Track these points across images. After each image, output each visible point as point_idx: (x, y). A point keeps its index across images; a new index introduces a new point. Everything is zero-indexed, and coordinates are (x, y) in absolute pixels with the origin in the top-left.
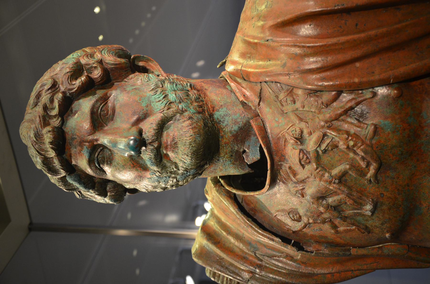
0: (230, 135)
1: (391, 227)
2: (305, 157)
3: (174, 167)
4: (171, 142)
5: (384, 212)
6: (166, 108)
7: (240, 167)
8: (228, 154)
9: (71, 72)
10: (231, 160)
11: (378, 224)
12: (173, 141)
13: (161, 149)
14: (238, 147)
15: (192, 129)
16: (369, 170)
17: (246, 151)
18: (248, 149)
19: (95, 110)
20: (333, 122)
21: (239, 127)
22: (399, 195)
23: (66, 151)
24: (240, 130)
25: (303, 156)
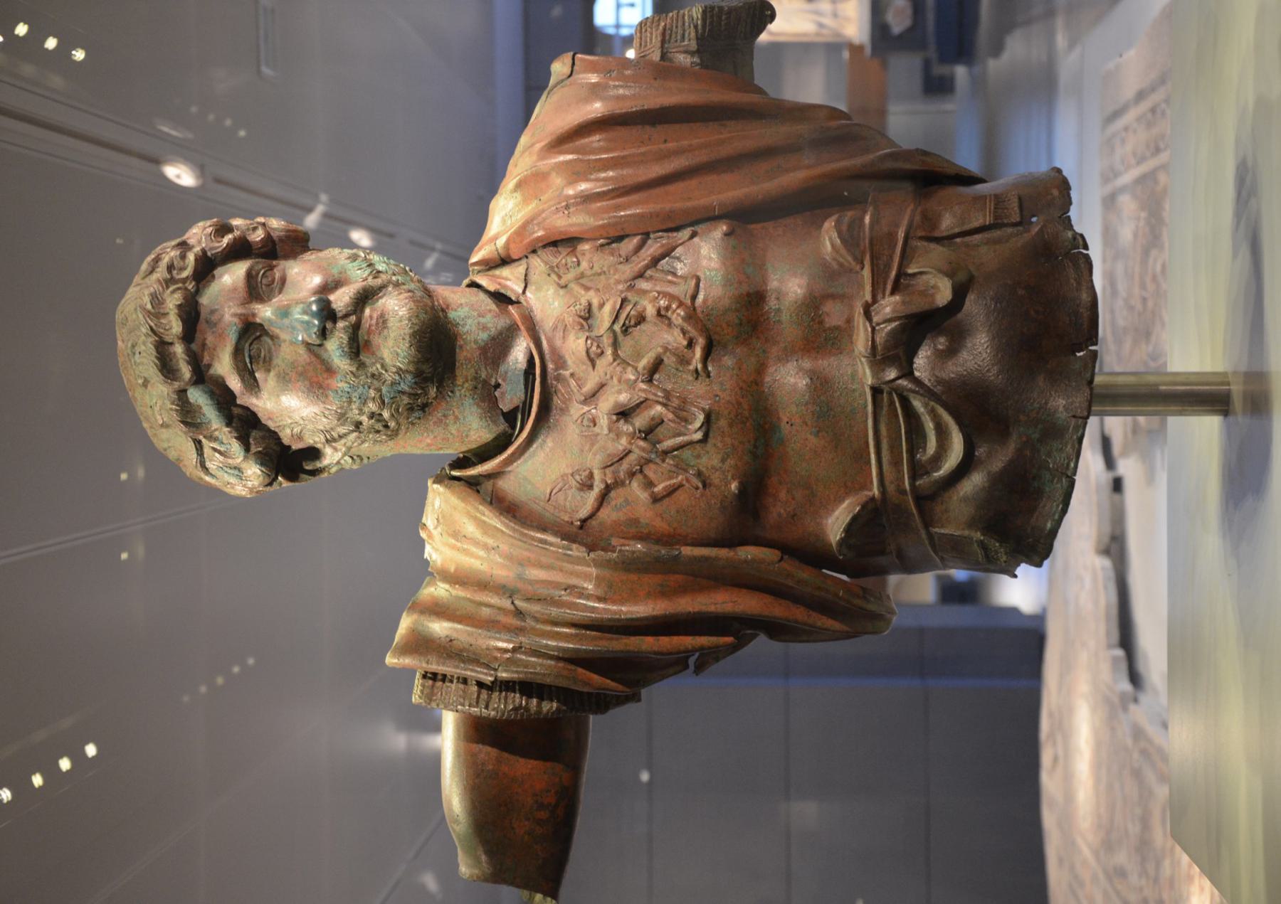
0: (475, 346)
1: (736, 465)
2: (595, 344)
3: (379, 366)
5: (723, 432)
6: (370, 278)
8: (470, 382)
9: (216, 225)
10: (473, 397)
11: (716, 462)
13: (360, 332)
14: (488, 372)
15: (414, 301)
16: (694, 352)
18: (504, 380)
19: (254, 273)
20: (636, 281)
21: (489, 336)
22: (743, 398)
23: (198, 335)
24: (491, 340)
25: (592, 344)
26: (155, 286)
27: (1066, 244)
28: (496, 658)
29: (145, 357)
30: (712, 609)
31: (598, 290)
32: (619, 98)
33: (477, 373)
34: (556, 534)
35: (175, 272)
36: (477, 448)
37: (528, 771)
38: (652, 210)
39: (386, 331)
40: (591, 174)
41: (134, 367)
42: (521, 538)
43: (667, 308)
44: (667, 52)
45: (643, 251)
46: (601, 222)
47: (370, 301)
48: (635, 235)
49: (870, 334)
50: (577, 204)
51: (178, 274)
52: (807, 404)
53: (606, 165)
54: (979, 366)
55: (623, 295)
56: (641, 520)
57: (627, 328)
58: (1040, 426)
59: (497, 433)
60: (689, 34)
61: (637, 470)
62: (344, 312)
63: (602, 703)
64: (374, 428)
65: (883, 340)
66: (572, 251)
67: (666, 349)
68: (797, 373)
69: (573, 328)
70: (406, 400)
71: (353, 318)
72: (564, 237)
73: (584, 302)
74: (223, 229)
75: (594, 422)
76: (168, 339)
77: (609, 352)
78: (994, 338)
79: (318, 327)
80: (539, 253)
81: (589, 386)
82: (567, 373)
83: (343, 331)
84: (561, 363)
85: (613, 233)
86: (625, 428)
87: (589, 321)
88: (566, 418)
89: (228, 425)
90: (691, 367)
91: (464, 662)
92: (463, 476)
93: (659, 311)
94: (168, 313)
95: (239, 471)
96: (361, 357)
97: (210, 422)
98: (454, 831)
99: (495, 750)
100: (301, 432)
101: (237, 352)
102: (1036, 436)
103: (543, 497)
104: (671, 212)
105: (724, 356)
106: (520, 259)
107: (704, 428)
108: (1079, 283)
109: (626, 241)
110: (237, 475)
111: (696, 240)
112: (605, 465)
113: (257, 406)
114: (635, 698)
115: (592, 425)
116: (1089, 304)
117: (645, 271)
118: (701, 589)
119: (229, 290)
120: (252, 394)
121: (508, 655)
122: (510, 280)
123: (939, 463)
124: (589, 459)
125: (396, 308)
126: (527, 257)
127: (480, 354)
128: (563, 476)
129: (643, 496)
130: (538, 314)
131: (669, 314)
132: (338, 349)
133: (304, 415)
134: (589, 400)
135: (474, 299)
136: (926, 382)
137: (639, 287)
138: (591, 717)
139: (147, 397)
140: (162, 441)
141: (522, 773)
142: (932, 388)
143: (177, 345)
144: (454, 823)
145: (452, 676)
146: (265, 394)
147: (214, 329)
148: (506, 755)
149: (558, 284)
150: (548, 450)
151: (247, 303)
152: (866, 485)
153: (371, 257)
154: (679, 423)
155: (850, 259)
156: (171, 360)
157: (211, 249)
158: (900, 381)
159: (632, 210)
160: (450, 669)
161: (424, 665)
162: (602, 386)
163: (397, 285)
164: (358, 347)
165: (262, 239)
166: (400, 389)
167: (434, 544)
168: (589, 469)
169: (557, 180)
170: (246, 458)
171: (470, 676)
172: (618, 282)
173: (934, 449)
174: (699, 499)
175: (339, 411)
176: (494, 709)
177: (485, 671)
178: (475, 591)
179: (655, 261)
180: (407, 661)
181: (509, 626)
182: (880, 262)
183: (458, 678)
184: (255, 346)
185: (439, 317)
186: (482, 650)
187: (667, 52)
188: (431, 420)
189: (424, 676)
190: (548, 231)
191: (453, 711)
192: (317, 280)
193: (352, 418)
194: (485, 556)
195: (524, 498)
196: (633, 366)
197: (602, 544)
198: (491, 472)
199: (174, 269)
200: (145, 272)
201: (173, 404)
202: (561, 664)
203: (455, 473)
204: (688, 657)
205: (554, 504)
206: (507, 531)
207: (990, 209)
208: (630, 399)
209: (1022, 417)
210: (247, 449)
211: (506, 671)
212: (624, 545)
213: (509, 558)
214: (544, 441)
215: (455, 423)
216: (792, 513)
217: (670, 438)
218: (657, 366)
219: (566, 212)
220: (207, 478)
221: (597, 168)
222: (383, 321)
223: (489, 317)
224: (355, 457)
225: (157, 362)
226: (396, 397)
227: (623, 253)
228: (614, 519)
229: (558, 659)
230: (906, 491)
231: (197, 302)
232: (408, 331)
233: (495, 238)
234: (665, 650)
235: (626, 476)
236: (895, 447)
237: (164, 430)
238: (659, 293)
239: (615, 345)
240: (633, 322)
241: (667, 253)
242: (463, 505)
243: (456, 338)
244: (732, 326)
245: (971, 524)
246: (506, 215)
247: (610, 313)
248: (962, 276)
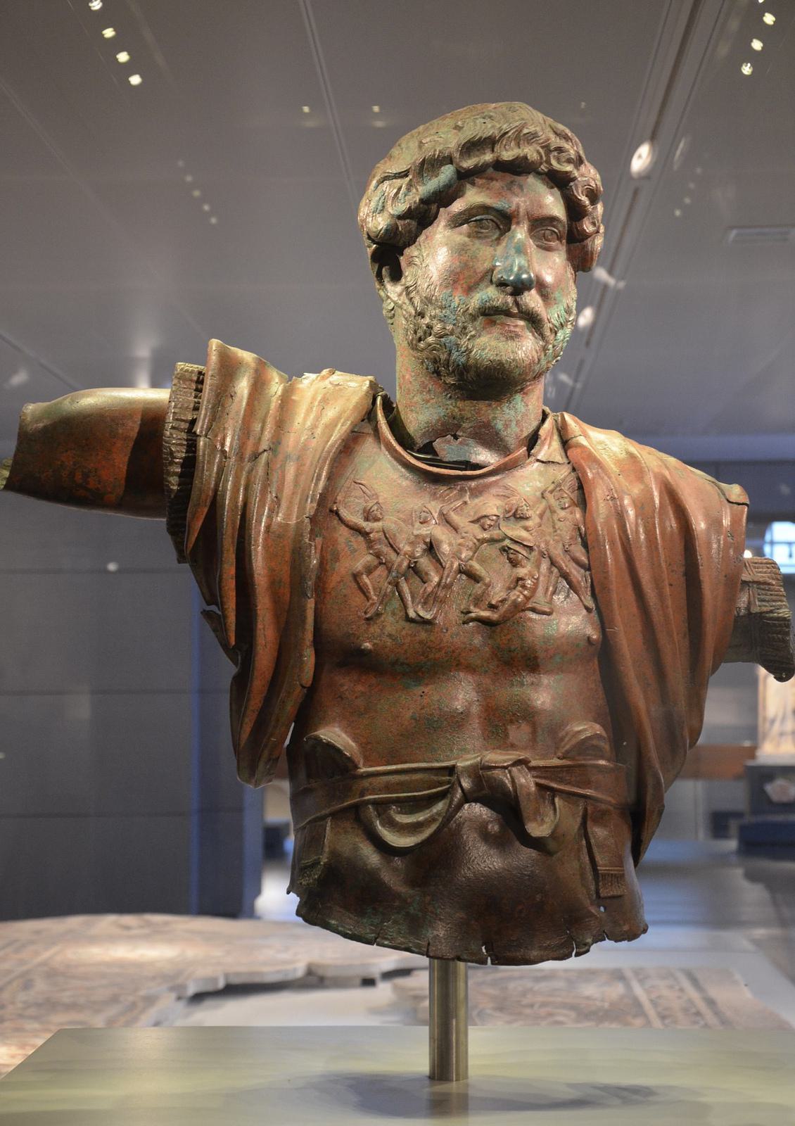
3: (473, 333)
6: (551, 326)
8: (459, 413)
11: (389, 629)
15: (530, 364)
17: (457, 439)
18: (461, 443)
20: (548, 559)
21: (500, 430)
25: (493, 520)
26: (543, 136)
27: (581, 937)
28: (216, 436)
29: (481, 128)
30: (260, 626)
31: (540, 526)
32: (709, 544)
33: (467, 419)
34: (326, 488)
35: (556, 153)
36: (401, 419)
37: (117, 464)
38: (610, 573)
39: (504, 339)
40: (642, 520)
41: (472, 118)
42: (322, 458)
43: (524, 587)
44: (749, 586)
45: (574, 565)
46: (599, 528)
47: (530, 325)
48: (588, 558)
49: (501, 765)
50: (615, 507)
51: (554, 156)
52: (441, 709)
53: (650, 533)
54: (473, 861)
55: (535, 548)
56: (337, 564)
57: (507, 552)
58: (420, 914)
60: (766, 606)
61: (382, 560)
62: (521, 302)
63: (177, 529)
65: (495, 776)
66: (574, 502)
67: (488, 585)
68: (467, 701)
70: (443, 357)
71: (515, 310)
72: (586, 496)
73: (530, 513)
74: (593, 196)
76: (497, 148)
77: (486, 535)
78: (497, 874)
79: (507, 280)
80: (572, 474)
81: (455, 517)
82: (467, 498)
83: (504, 302)
84: (476, 493)
85: (590, 539)
86: (418, 549)
87: (512, 518)
88: (427, 497)
89: (421, 200)
90: (472, 608)
91: (213, 408)
92: (376, 408)
93: (521, 579)
94: (519, 148)
95: (381, 210)
96: (481, 318)
97: (425, 185)
98: (64, 399)
99: (135, 435)
100: (415, 264)
101: (485, 209)
102: (412, 911)
103: (358, 477)
104: (609, 589)
105: (482, 636)
106: (567, 457)
107: (419, 618)
108: (546, 948)
109: (583, 550)
111: (584, 612)
113: (438, 226)
114: (182, 558)
116: (528, 957)
117: (556, 567)
118: (277, 616)
119: (540, 201)
120: (449, 221)
121: (219, 446)
122: (549, 448)
123: (387, 825)
125: (524, 348)
126: (569, 463)
128: (377, 495)
129: (359, 565)
130: (519, 473)
131: (519, 588)
133: (430, 268)
134: (443, 518)
135: (532, 417)
136: (459, 814)
137: (543, 562)
138: (165, 520)
139: (446, 129)
140: (408, 142)
141: (115, 459)
142: (454, 819)
143: (491, 155)
144: (71, 399)
145: (200, 398)
146: (448, 233)
147: (505, 188)
148: (131, 444)
149: (545, 491)
150: (400, 482)
151: (529, 218)
152: (368, 761)
153: (569, 326)
154: (423, 597)
155: (568, 747)
156: (478, 150)
157: (576, 186)
158: (460, 791)
159: (611, 556)
160: (206, 395)
161: (210, 373)
162: (456, 529)
163: (545, 349)
164: (490, 314)
165: (585, 230)
166: (453, 352)
167: (316, 382)
169: (636, 490)
170: (392, 216)
171: (201, 414)
172: (547, 543)
173: (400, 821)
174: (357, 614)
175: (433, 298)
176: (171, 434)
177: (205, 427)
178: (275, 418)
179: (565, 576)
180: (214, 358)
181: (244, 447)
182: (564, 774)
183: (199, 403)
184: (491, 224)
185: (516, 386)
186: (223, 424)
187: (749, 586)
189: (200, 373)
190: (592, 482)
191: (170, 398)
192: (549, 279)
194: (307, 426)
195: (357, 460)
196: (473, 556)
197: (317, 529)
198: (380, 432)
199: (559, 153)
200: (556, 128)
201: (440, 152)
202: (211, 493)
203: (379, 400)
204: (217, 605)
206: (328, 446)
207: (611, 870)
209: (428, 898)
210: (400, 217)
211: (205, 444)
212: (315, 549)
213: (305, 448)
214: (407, 479)
216: (343, 696)
217: (410, 589)
218: (473, 577)
219: (608, 498)
220: (374, 182)
221: (647, 524)
222: (513, 336)
223: (517, 430)
224: (393, 312)
227: (572, 548)
228: (339, 540)
229: (216, 491)
230: (363, 796)
231: (529, 173)
232: (504, 358)
233: (586, 436)
234: (223, 584)
235: (376, 551)
236: (402, 786)
237: (417, 144)
238: (537, 579)
239: (492, 541)
240: (511, 556)
241: (572, 586)
242: (351, 407)
243: (498, 401)
244: (508, 644)
245: (334, 854)
246: (606, 445)
247: (520, 536)
248: (552, 845)
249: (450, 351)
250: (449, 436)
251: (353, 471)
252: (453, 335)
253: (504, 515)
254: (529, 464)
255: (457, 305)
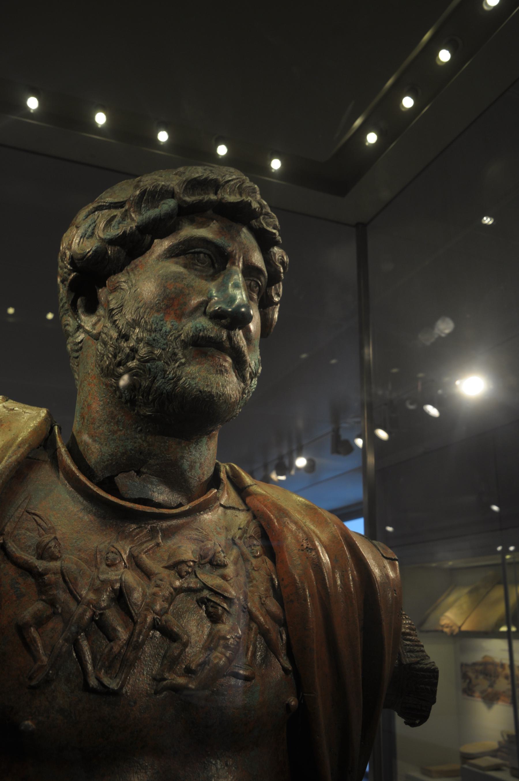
3: (183, 360)
4: (224, 366)
7: (112, 463)
12: (225, 369)
13: (213, 349)
21: (185, 471)
25: (190, 567)
36: (79, 451)
43: (227, 647)
55: (236, 600)
59: (95, 469)
64: (119, 353)
69: (201, 549)
70: (145, 384)
71: (227, 345)
73: (227, 560)
75: (111, 565)
80: (254, 521)
84: (168, 533)
96: (191, 347)
100: (121, 289)
110: (86, 234)
112: (65, 574)
115: (108, 563)
117: (256, 622)
124: (71, 556)
127: (171, 460)
132: (203, 326)
134: (133, 560)
150: (81, 515)
166: (158, 378)
168: (61, 557)
170: (102, 240)
175: (143, 320)
184: (208, 260)
188: (115, 409)
193: (134, 332)
205: (24, 517)
208: (135, 604)
210: (112, 242)
215: (110, 431)
224: (80, 345)
225: (203, 177)
226: (150, 374)
232: (214, 391)
239: (189, 590)
240: (211, 609)
249: (155, 378)
250: (133, 472)
251: (26, 499)
252: (160, 361)
253: (199, 561)
254: (215, 508)
255: (168, 330)
